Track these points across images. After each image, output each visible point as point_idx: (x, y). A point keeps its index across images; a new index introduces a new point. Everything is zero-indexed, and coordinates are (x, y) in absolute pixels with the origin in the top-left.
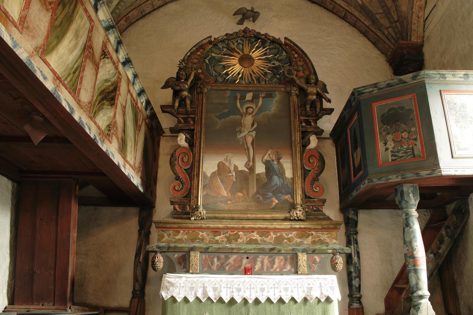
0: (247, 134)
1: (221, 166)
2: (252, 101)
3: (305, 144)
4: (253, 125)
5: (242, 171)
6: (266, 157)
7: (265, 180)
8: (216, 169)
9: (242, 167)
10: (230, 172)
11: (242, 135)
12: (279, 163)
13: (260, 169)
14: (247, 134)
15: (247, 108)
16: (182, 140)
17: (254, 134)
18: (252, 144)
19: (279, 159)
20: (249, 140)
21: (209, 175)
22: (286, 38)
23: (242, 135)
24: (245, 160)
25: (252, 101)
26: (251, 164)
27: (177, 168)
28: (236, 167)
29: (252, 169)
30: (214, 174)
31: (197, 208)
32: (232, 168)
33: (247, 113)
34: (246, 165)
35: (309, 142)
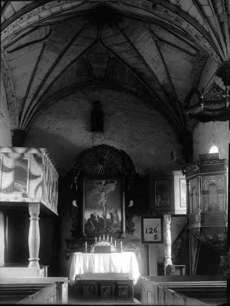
0: (103, 200)
1: (92, 215)
2: (105, 185)
3: (127, 203)
4: (105, 197)
5: (101, 218)
6: (111, 212)
7: (111, 222)
8: (89, 217)
9: (101, 216)
10: (95, 218)
11: (101, 201)
12: (117, 214)
13: (108, 217)
14: (103, 200)
15: (103, 189)
16: (74, 203)
17: (105, 201)
18: (105, 205)
19: (116, 212)
20: (104, 204)
21: (87, 219)
22: (121, 150)
23: (101, 201)
24: (102, 213)
25: (105, 185)
26: (105, 214)
27: (73, 216)
28: (98, 216)
29: (105, 217)
30: (89, 219)
31: (83, 234)
32: (97, 216)
33: (103, 191)
34: (103, 215)
35: (129, 204)
